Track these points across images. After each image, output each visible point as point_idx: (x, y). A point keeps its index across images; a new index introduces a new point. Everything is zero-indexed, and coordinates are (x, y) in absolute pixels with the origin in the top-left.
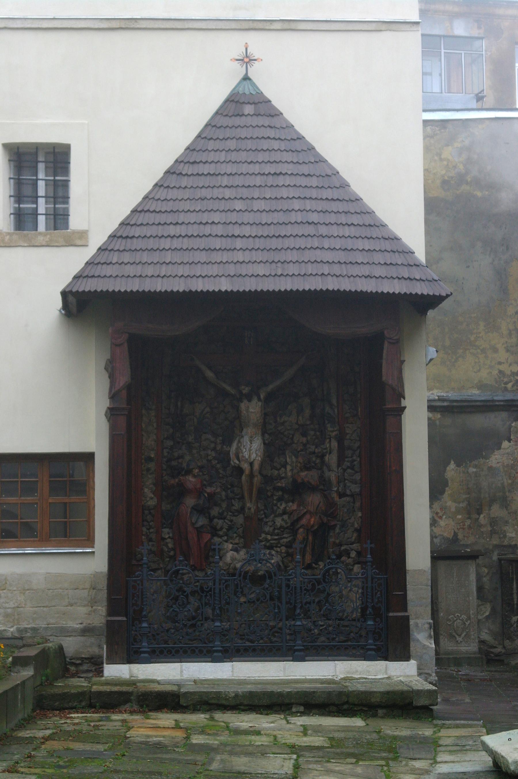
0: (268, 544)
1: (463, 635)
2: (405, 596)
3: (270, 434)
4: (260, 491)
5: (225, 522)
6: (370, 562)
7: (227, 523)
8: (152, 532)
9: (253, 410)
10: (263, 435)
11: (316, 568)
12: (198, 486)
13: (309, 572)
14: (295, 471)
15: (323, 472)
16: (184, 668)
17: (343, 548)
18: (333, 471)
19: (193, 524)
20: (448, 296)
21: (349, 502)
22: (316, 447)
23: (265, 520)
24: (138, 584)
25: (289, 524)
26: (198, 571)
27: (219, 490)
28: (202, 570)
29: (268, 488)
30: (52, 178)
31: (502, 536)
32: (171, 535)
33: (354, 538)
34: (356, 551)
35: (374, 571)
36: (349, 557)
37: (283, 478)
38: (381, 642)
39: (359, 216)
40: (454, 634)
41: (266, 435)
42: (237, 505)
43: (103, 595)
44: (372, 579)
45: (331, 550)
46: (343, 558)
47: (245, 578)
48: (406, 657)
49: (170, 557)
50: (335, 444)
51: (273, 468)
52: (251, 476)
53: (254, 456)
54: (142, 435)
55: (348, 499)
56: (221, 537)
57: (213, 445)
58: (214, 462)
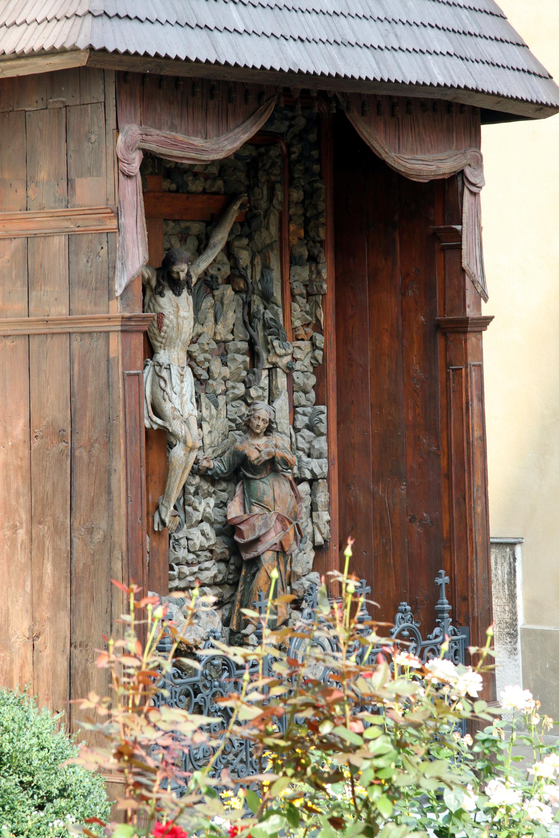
0: (182, 584)
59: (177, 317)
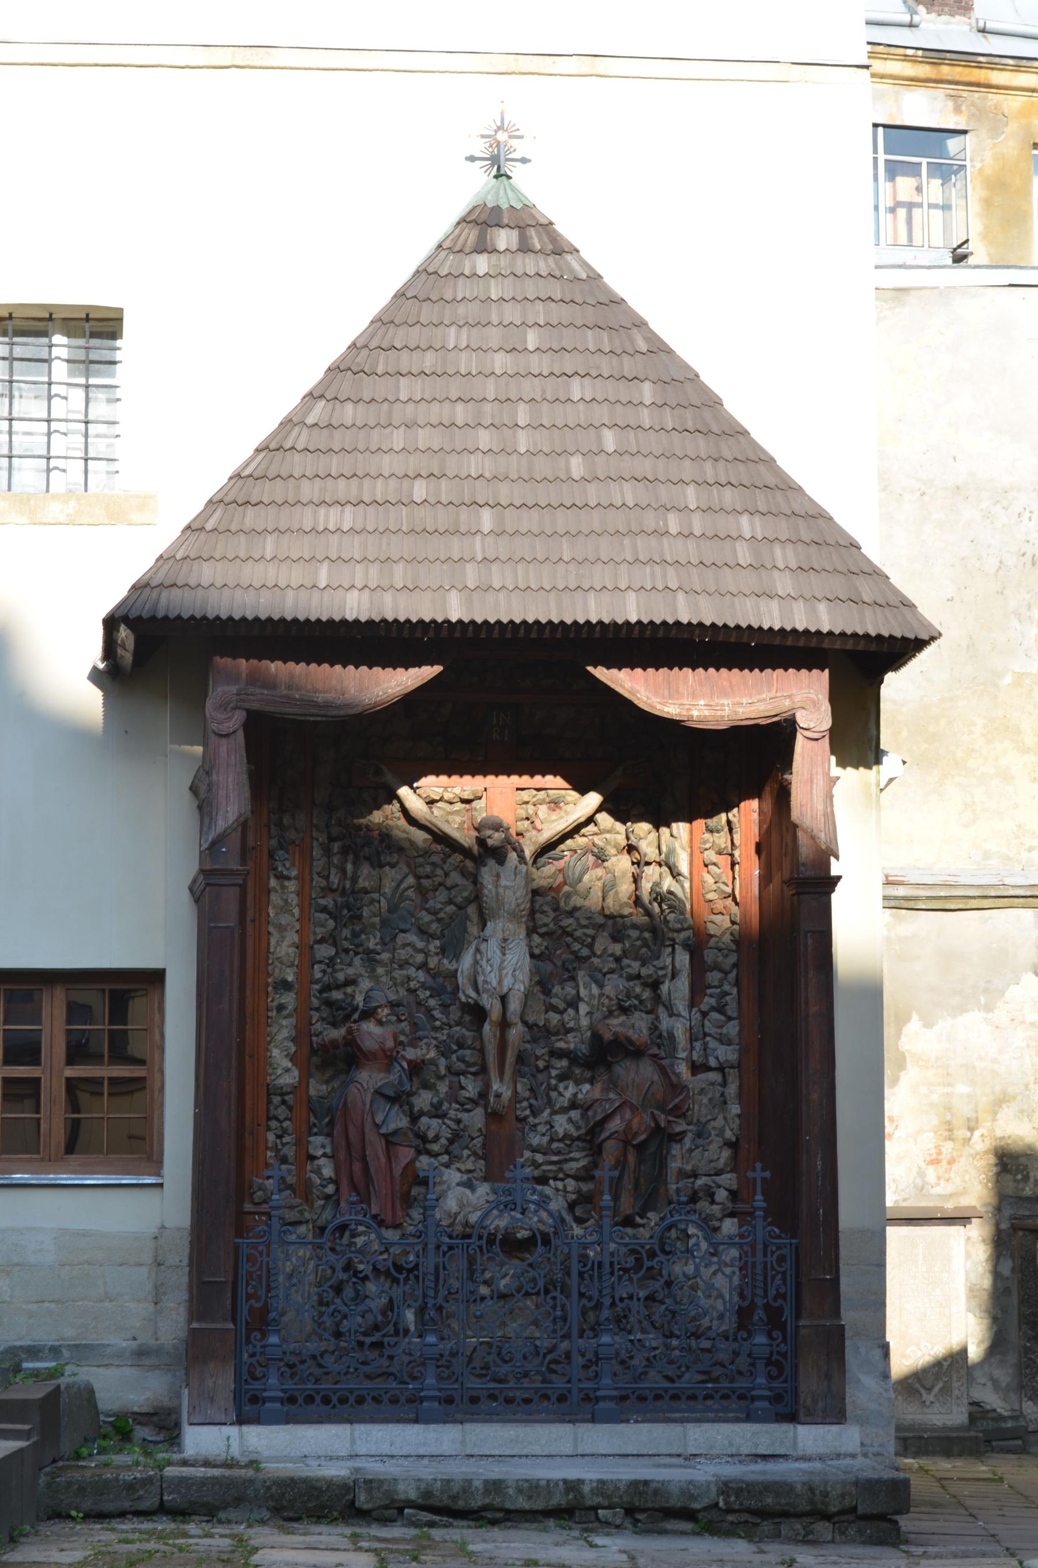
0: (537, 1173)
1: (936, 1389)
2: (836, 1282)
3: (541, 935)
4: (521, 1058)
5: (444, 1123)
6: (760, 1209)
7: (448, 1126)
8: (287, 1143)
9: (508, 884)
10: (529, 935)
11: (643, 1226)
12: (390, 1043)
13: (629, 1230)
14: (597, 1015)
15: (657, 1018)
16: (357, 1434)
17: (700, 1182)
18: (679, 1015)
19: (378, 1126)
20: (933, 639)
21: (712, 1084)
22: (643, 965)
23: (531, 1120)
24: (261, 1254)
25: (583, 1131)
26: (387, 1228)
27: (432, 1054)
28: (397, 1226)
29: (539, 1052)
30: (82, 381)
31: (1019, 1177)
32: (328, 1150)
33: (722, 1161)
34: (726, 1189)
35: (769, 1228)
36: (713, 1202)
37: (569, 1031)
38: (785, 1381)
39: (741, 467)
40: (917, 1386)
41: (536, 937)
42: (471, 1087)
43: (180, 1279)
44: (766, 1246)
45: (674, 1187)
46: (703, 1205)
47: (491, 1241)
48: (836, 1414)
49: (327, 1197)
50: (683, 959)
51: (551, 1008)
52: (504, 1024)
53: (507, 982)
54: (269, 933)
55: (714, 1076)
56: (436, 1155)
57: (420, 958)
58: (423, 994)
59: (497, 887)
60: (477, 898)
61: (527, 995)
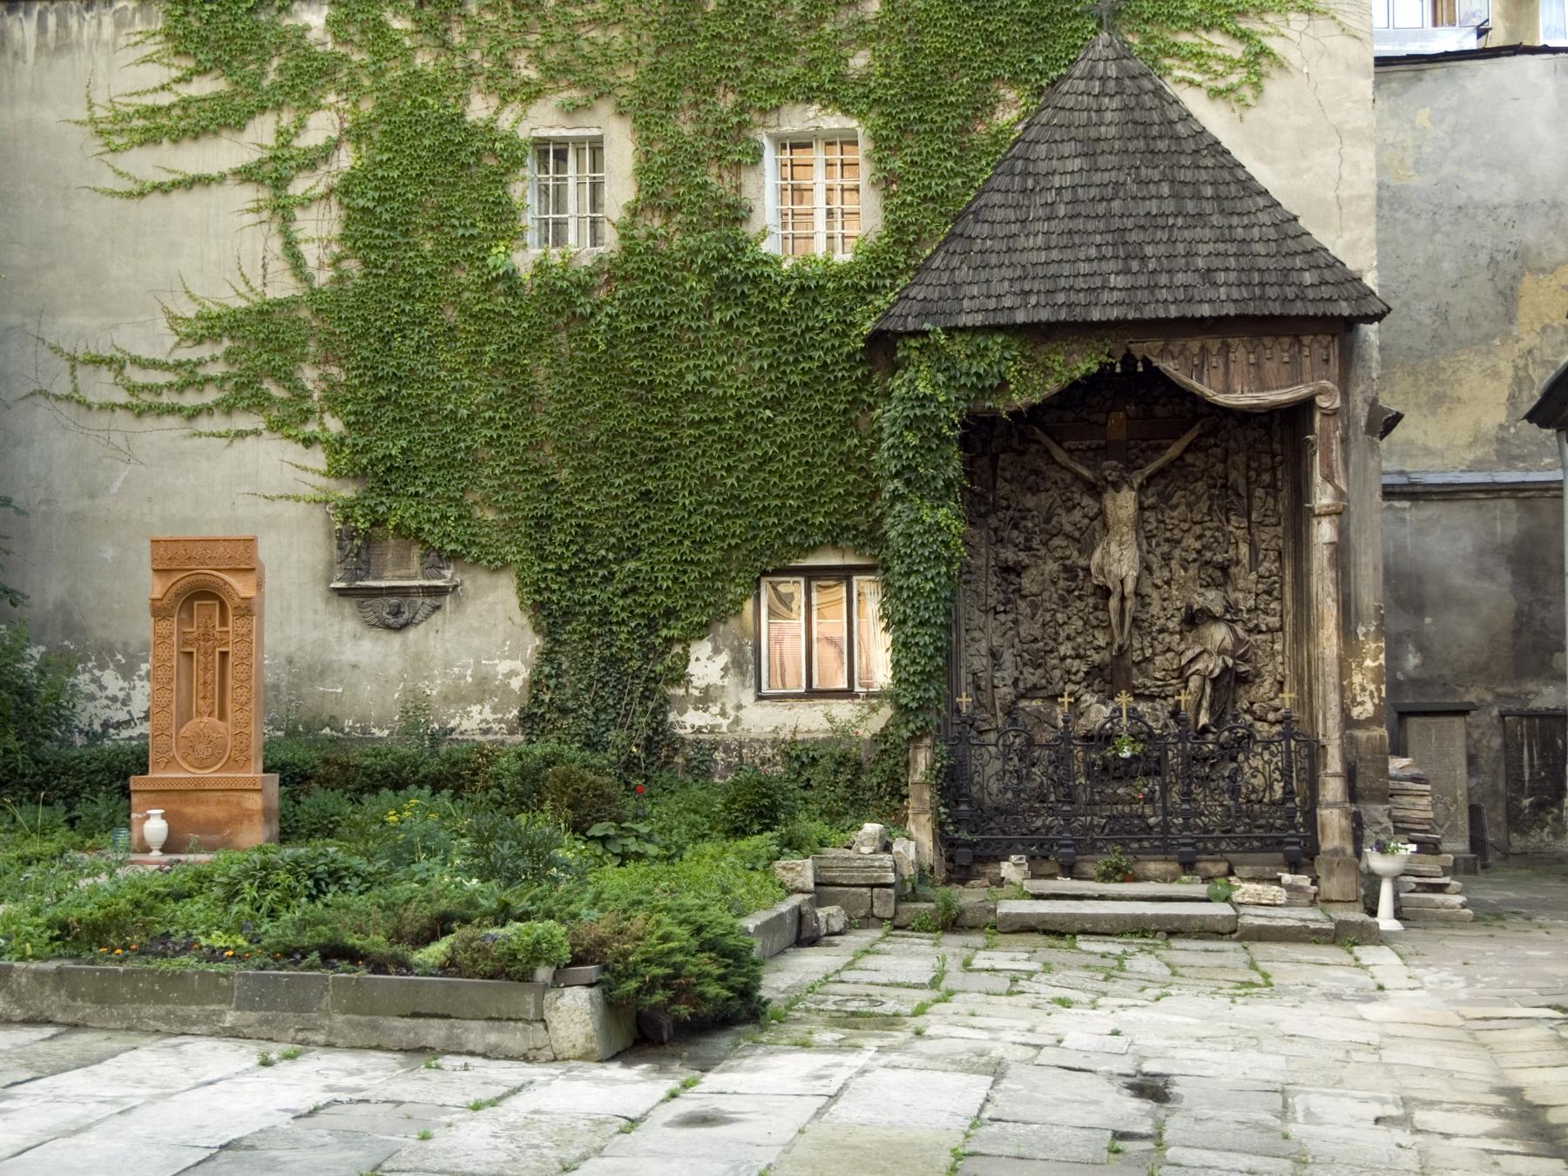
4: (1134, 620)
50: (1244, 549)
52: (1123, 598)
60: (1102, 512)
61: (1138, 579)
